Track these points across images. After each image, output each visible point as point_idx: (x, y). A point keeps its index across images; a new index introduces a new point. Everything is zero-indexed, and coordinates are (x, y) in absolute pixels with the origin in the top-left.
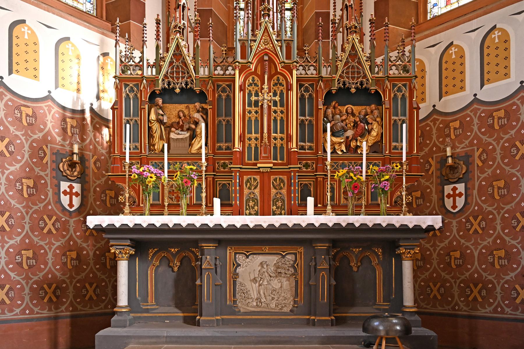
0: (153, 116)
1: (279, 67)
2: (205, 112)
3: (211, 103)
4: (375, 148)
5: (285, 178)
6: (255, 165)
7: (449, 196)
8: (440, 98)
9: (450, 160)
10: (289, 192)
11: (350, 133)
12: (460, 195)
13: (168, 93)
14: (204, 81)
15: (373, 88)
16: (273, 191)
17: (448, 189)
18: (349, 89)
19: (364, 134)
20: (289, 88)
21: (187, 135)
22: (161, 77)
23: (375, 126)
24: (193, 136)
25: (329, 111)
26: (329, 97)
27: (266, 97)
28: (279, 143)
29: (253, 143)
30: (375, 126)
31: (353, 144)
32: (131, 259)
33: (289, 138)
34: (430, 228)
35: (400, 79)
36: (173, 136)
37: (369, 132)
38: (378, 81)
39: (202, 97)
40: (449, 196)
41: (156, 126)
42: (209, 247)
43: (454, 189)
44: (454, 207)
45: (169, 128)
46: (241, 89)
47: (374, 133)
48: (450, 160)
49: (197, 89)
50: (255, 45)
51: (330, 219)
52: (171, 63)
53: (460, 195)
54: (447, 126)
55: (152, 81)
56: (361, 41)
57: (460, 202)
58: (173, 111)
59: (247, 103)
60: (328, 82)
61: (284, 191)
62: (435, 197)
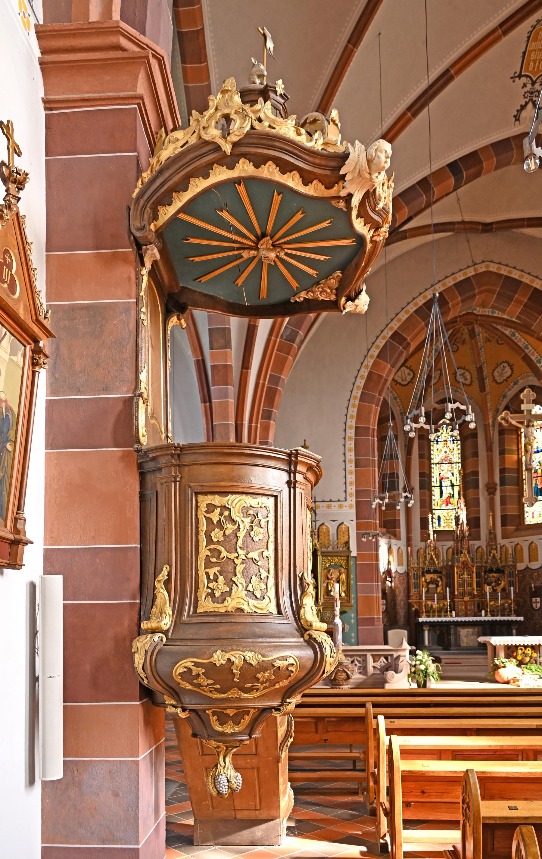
0: (423, 580)
1: (470, 566)
2: (441, 577)
3: (444, 575)
4: (503, 590)
5: (473, 603)
6: (463, 598)
7: (534, 602)
8: (530, 562)
9: (533, 589)
10: (474, 607)
11: (493, 584)
12: (538, 602)
13: (428, 572)
14: (441, 568)
15: (502, 569)
16: (469, 607)
17: (534, 599)
18: (492, 569)
19: (499, 584)
20: (473, 572)
21: (434, 586)
22: (426, 567)
23: (503, 582)
24: (437, 586)
25: (486, 576)
26: (485, 572)
27: (466, 576)
28: (470, 591)
29: (461, 591)
30: (503, 582)
31: (495, 588)
32: (429, 631)
33: (473, 589)
34: (520, 621)
35: (512, 565)
36: (430, 586)
37: (500, 584)
38: (503, 566)
39: (441, 573)
40: (534, 602)
41: (424, 583)
42: (452, 627)
43: (536, 600)
44: (536, 607)
45: (428, 584)
46: (457, 573)
47: (502, 584)
48: (533, 589)
49: (439, 571)
50: (461, 559)
51: (490, 618)
52: (429, 561)
53: (538, 602)
54: (532, 574)
55: (423, 568)
56: (497, 553)
57: (539, 605)
58: (428, 577)
59: (459, 577)
60: (486, 567)
61: (473, 607)
62: (529, 602)
